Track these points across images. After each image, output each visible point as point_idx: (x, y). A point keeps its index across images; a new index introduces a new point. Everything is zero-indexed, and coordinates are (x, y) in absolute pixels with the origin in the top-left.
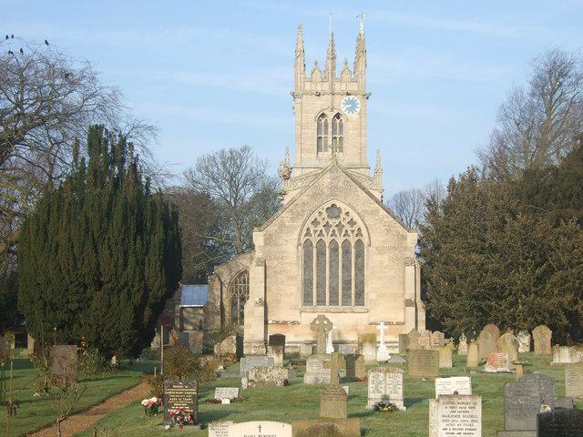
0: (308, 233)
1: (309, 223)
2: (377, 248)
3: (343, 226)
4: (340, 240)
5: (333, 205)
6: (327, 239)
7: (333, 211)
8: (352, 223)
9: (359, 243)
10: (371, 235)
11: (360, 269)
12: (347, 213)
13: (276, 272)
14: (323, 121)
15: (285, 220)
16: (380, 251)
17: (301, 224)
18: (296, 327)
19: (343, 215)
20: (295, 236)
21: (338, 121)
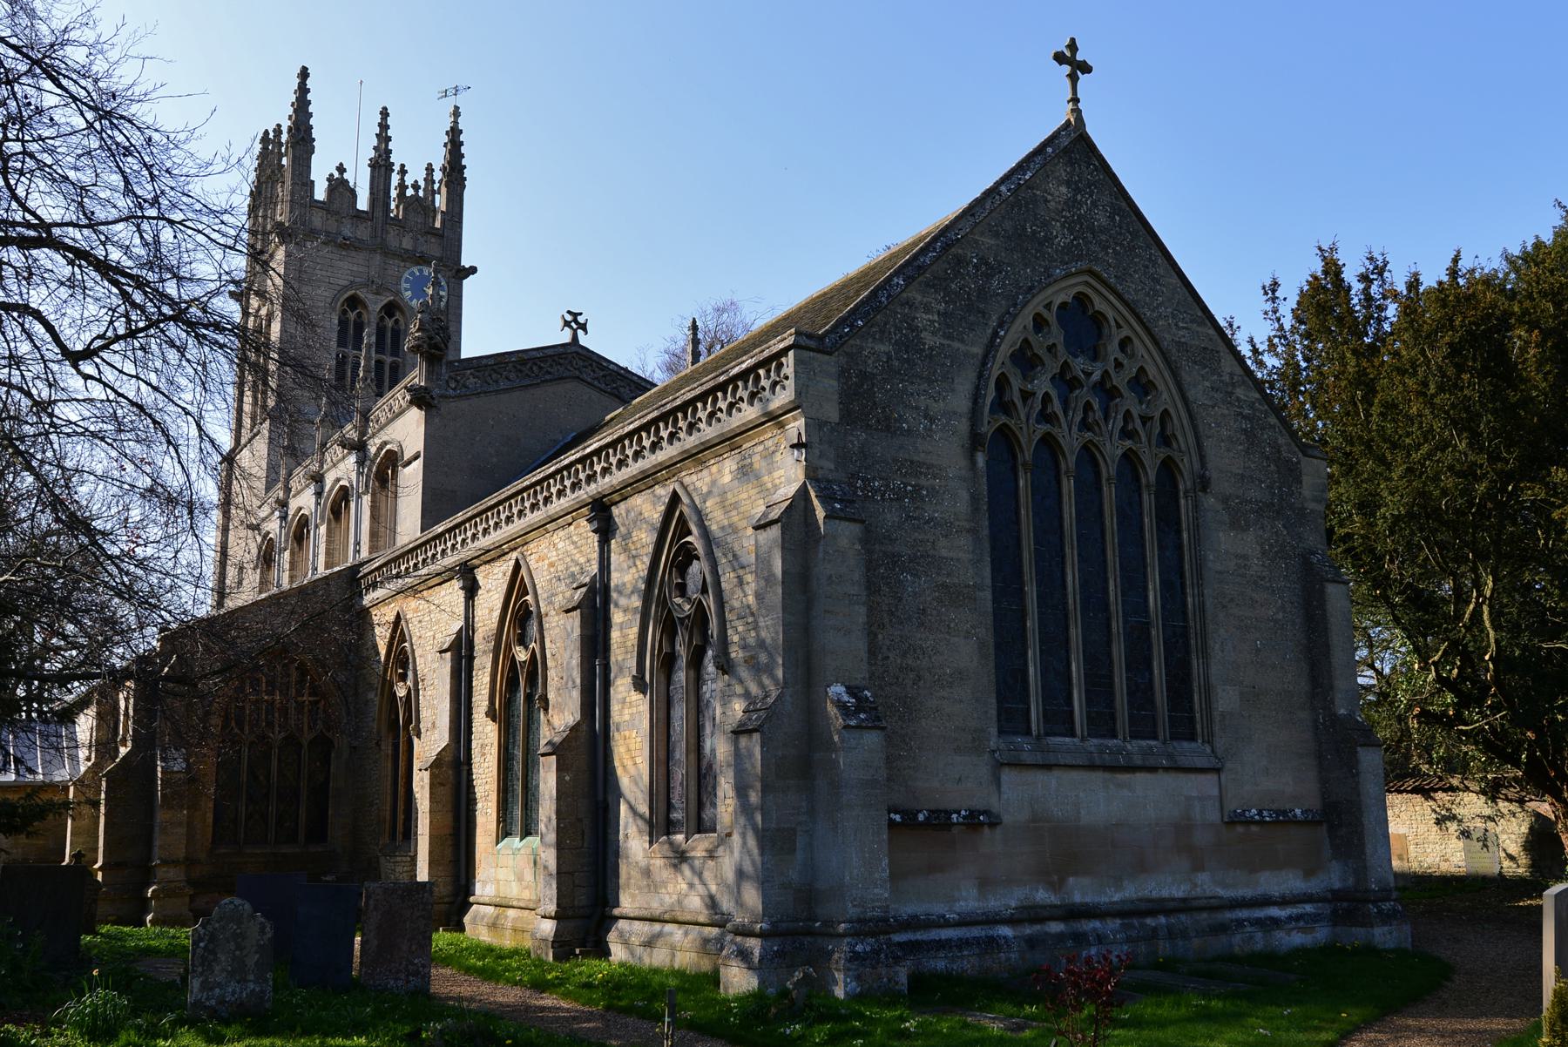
0: (1003, 405)
1: (1004, 351)
2: (1225, 500)
4: (1112, 449)
5: (1081, 299)
6: (1071, 440)
8: (1142, 385)
9: (1168, 468)
11: (1173, 588)
12: (1124, 344)
14: (352, 316)
15: (922, 318)
17: (977, 350)
18: (990, 841)
20: (960, 401)
21: (390, 323)
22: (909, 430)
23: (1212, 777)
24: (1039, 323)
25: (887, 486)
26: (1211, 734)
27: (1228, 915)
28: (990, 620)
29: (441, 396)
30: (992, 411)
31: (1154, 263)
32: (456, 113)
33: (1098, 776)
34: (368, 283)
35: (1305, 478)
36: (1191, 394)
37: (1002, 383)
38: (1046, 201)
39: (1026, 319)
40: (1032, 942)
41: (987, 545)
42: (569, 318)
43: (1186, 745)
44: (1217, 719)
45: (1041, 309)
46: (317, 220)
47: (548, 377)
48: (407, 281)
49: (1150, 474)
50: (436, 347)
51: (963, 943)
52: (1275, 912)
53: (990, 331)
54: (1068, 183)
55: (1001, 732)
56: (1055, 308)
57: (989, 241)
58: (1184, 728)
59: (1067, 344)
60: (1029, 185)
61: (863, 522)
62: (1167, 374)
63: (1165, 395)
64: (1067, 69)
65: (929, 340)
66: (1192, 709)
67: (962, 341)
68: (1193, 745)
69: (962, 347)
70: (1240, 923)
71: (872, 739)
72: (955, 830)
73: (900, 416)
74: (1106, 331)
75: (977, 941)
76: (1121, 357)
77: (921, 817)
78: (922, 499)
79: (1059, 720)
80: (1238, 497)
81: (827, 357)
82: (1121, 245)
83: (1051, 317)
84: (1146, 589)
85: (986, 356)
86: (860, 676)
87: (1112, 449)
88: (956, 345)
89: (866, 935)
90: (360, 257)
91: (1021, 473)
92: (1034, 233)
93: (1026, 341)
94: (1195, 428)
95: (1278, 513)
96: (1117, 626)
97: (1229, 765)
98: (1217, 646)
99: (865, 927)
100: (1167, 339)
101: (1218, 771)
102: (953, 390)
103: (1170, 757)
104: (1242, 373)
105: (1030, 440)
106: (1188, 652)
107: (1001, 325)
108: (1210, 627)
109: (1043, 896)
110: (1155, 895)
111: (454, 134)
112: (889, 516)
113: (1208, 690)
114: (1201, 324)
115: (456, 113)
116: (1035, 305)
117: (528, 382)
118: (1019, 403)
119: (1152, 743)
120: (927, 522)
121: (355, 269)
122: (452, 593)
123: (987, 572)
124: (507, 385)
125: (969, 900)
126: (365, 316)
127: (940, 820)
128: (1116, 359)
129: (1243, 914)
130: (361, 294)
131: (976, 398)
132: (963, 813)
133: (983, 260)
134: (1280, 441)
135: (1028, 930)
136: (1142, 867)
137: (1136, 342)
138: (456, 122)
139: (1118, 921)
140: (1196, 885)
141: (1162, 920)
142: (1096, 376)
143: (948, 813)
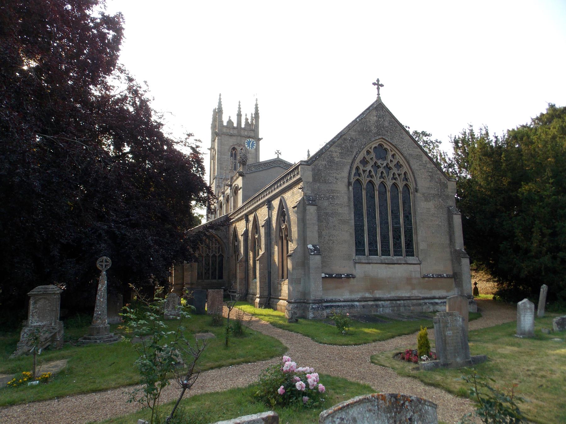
2: (423, 194)
3: (390, 168)
4: (389, 183)
5: (381, 145)
6: (377, 182)
7: (381, 151)
8: (398, 166)
10: (418, 180)
11: (407, 217)
12: (393, 156)
13: (327, 214)
14: (234, 152)
15: (335, 154)
16: (427, 198)
17: (350, 161)
19: (390, 157)
20: (345, 174)
22: (331, 182)
23: (419, 266)
24: (368, 152)
25: (325, 196)
26: (418, 255)
27: (422, 301)
28: (354, 228)
29: (246, 173)
30: (355, 175)
31: (402, 134)
32: (257, 100)
33: (384, 265)
34: (237, 144)
35: (449, 187)
36: (413, 168)
37: (357, 168)
38: (370, 121)
39: (364, 152)
40: (364, 306)
41: (353, 210)
42: (277, 152)
43: (411, 257)
44: (420, 251)
45: (369, 149)
46: (224, 130)
47: (272, 167)
48: (246, 142)
49: (401, 188)
50: (244, 162)
51: (344, 306)
52: (437, 301)
53: (353, 156)
54: (376, 116)
55: (356, 255)
56: (372, 148)
57: (353, 133)
58: (410, 252)
59: (376, 157)
60: (365, 118)
61: (317, 206)
62: (405, 162)
63: (405, 168)
64: (376, 86)
65: (336, 159)
66: (413, 248)
67: (346, 159)
68: (413, 257)
69: (346, 161)
70: (426, 303)
71: (318, 258)
72: (343, 279)
73: (329, 179)
74: (388, 153)
75: (349, 305)
76: (392, 159)
77: (334, 276)
78: (334, 199)
79: (373, 252)
80: (427, 193)
81: (309, 166)
82: (392, 130)
83: (372, 151)
84: (399, 218)
85: (352, 162)
86: (316, 242)
87: (389, 183)
88: (344, 160)
89: (316, 303)
90: (235, 138)
91: (363, 190)
92: (366, 130)
93: (364, 157)
94: (414, 176)
95: (440, 196)
96: (390, 228)
97: (423, 263)
98: (420, 232)
99: (316, 302)
100: (406, 154)
101: (420, 264)
102: (343, 172)
103: (405, 261)
104: (429, 160)
105: (365, 182)
106: (412, 234)
107: (356, 154)
108: (418, 227)
109: (367, 295)
110: (400, 295)
111: (256, 105)
112: (325, 203)
113: (417, 243)
114: (417, 148)
115: (257, 100)
116: (367, 148)
117: (266, 168)
118: (362, 173)
119: (400, 257)
120: (336, 204)
121: (234, 141)
122: (243, 222)
123: (353, 215)
124: (262, 169)
125: (347, 296)
126: (237, 152)
127: (339, 277)
128: (390, 160)
129: (426, 301)
130: (236, 147)
131: (350, 173)
132: (345, 275)
133: (352, 138)
134: (441, 177)
135: (363, 303)
136: (397, 288)
137: (396, 154)
138: (257, 102)
139: (389, 302)
140: (413, 293)
141: (402, 302)
142: (385, 165)
143: (341, 275)
